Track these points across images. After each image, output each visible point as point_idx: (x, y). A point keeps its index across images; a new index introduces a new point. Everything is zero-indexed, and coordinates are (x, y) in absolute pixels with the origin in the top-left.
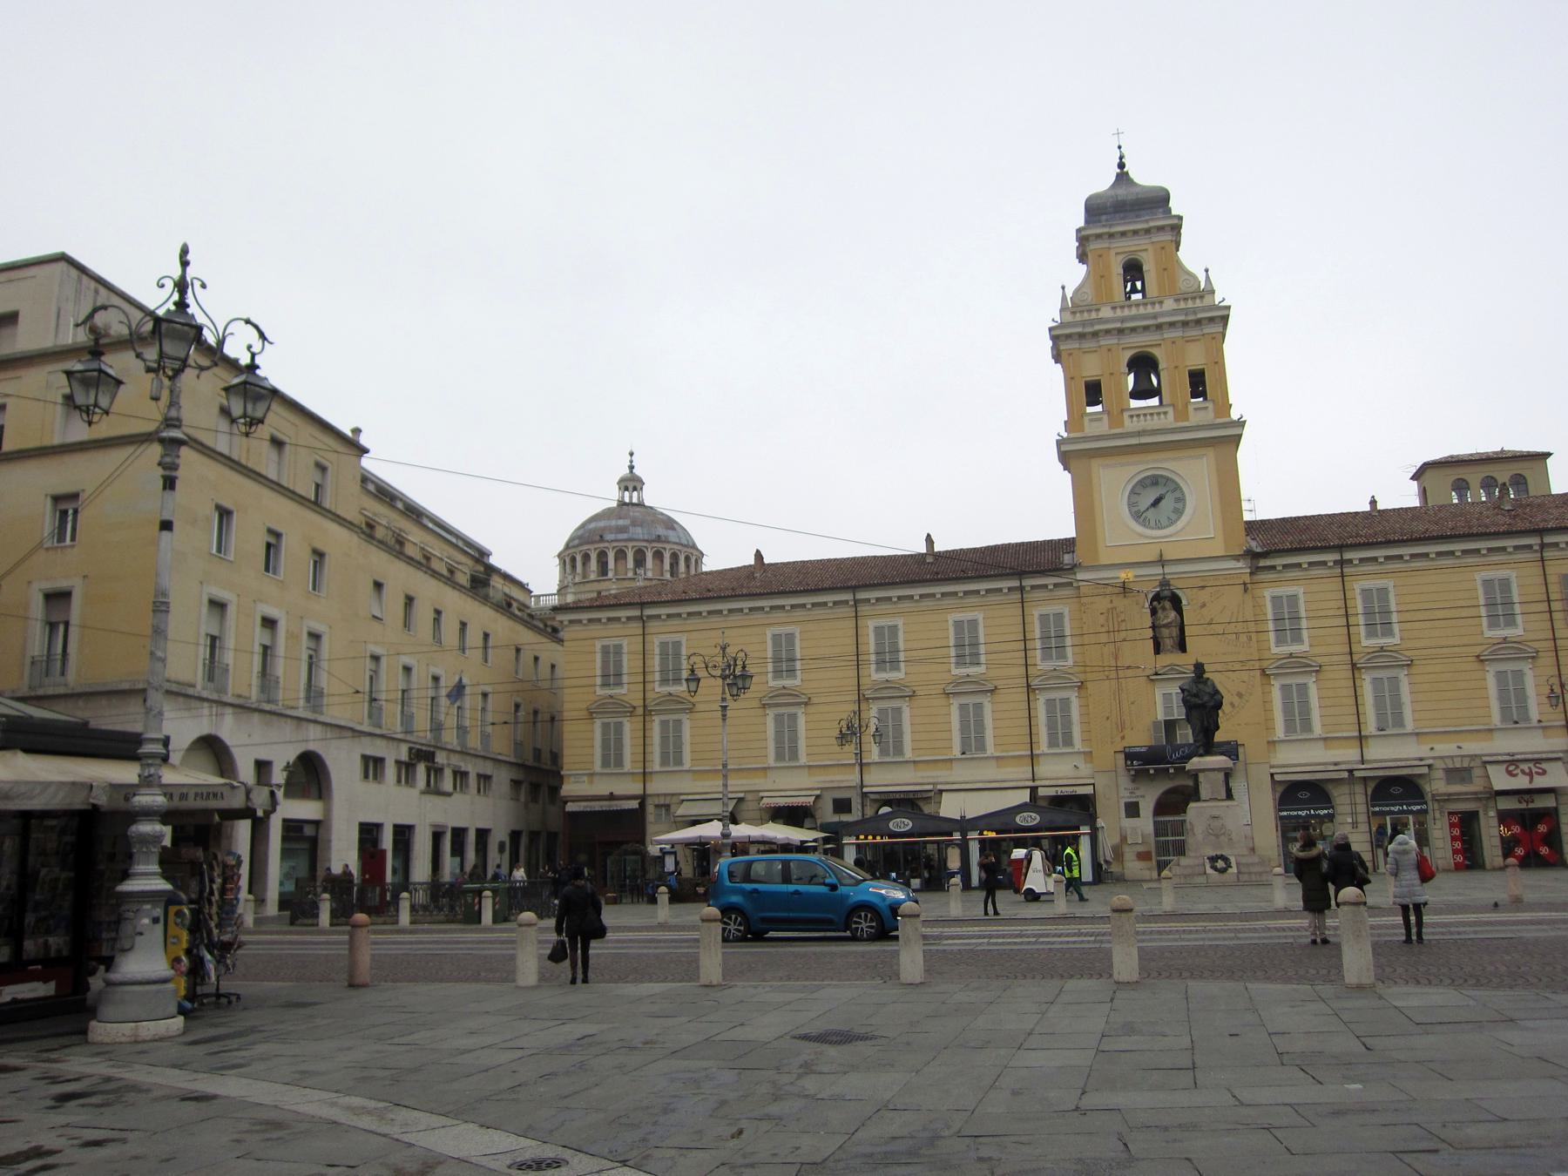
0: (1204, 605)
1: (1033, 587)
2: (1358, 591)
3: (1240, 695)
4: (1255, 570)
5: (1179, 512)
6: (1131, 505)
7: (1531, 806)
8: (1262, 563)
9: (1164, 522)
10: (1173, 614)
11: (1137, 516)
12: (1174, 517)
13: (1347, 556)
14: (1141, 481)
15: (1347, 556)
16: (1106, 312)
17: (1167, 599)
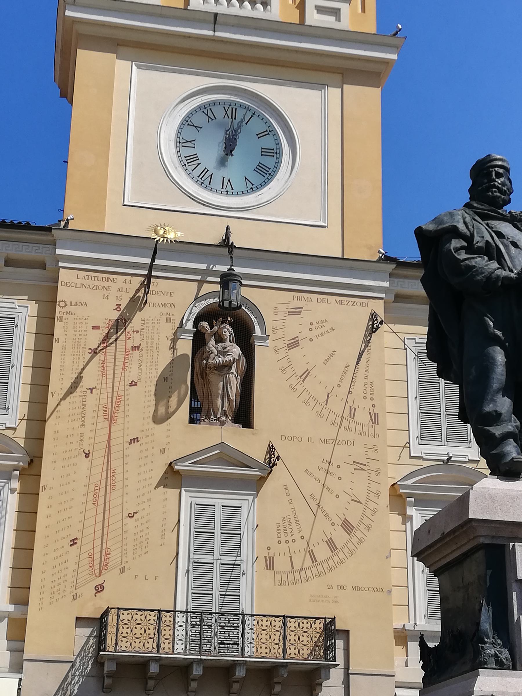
0: (294, 344)
3: (347, 527)
5: (266, 173)
6: (182, 142)
9: (238, 184)
10: (236, 351)
11: (189, 162)
12: (256, 179)
14: (204, 108)
17: (227, 319)
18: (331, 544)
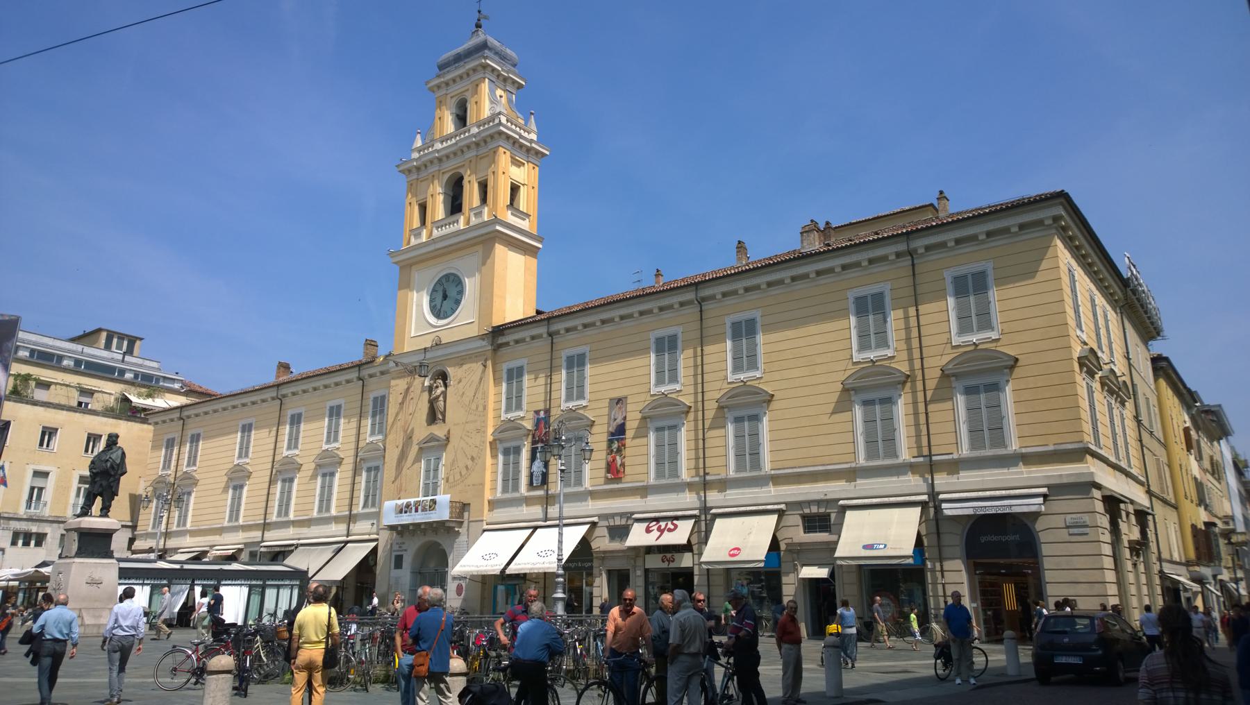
1: (371, 376)
2: (564, 358)
4: (497, 348)
7: (672, 565)
8: (501, 340)
10: (442, 389)
13: (554, 328)
15: (554, 328)
16: (438, 146)
18: (467, 467)
